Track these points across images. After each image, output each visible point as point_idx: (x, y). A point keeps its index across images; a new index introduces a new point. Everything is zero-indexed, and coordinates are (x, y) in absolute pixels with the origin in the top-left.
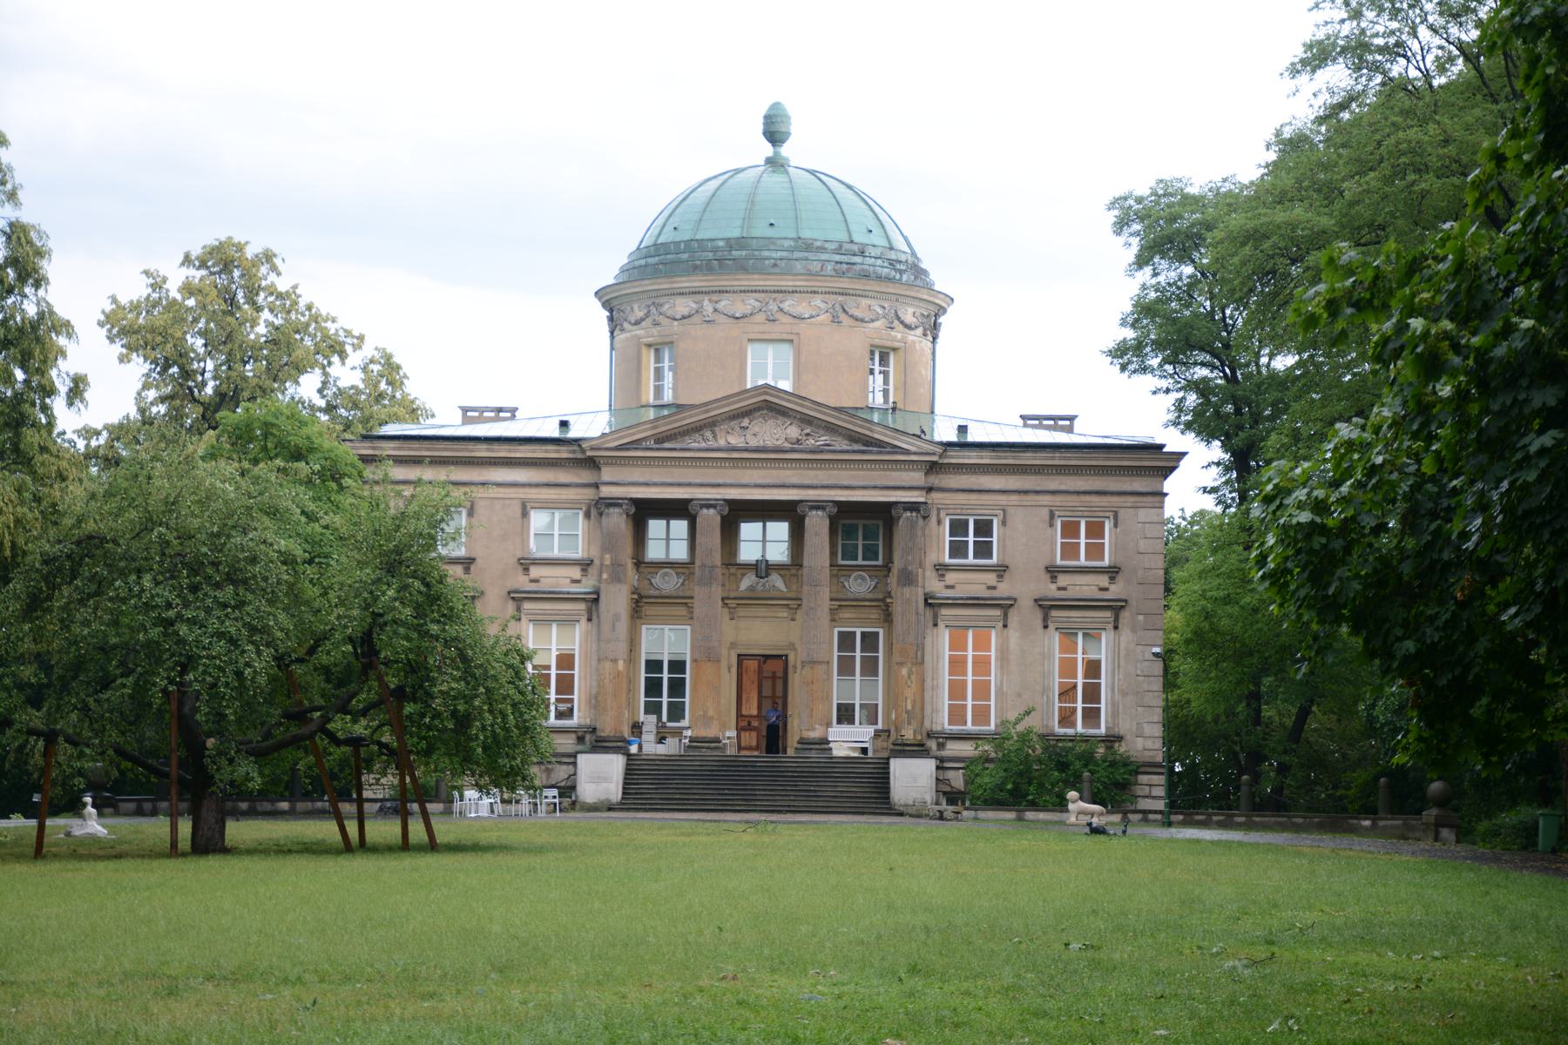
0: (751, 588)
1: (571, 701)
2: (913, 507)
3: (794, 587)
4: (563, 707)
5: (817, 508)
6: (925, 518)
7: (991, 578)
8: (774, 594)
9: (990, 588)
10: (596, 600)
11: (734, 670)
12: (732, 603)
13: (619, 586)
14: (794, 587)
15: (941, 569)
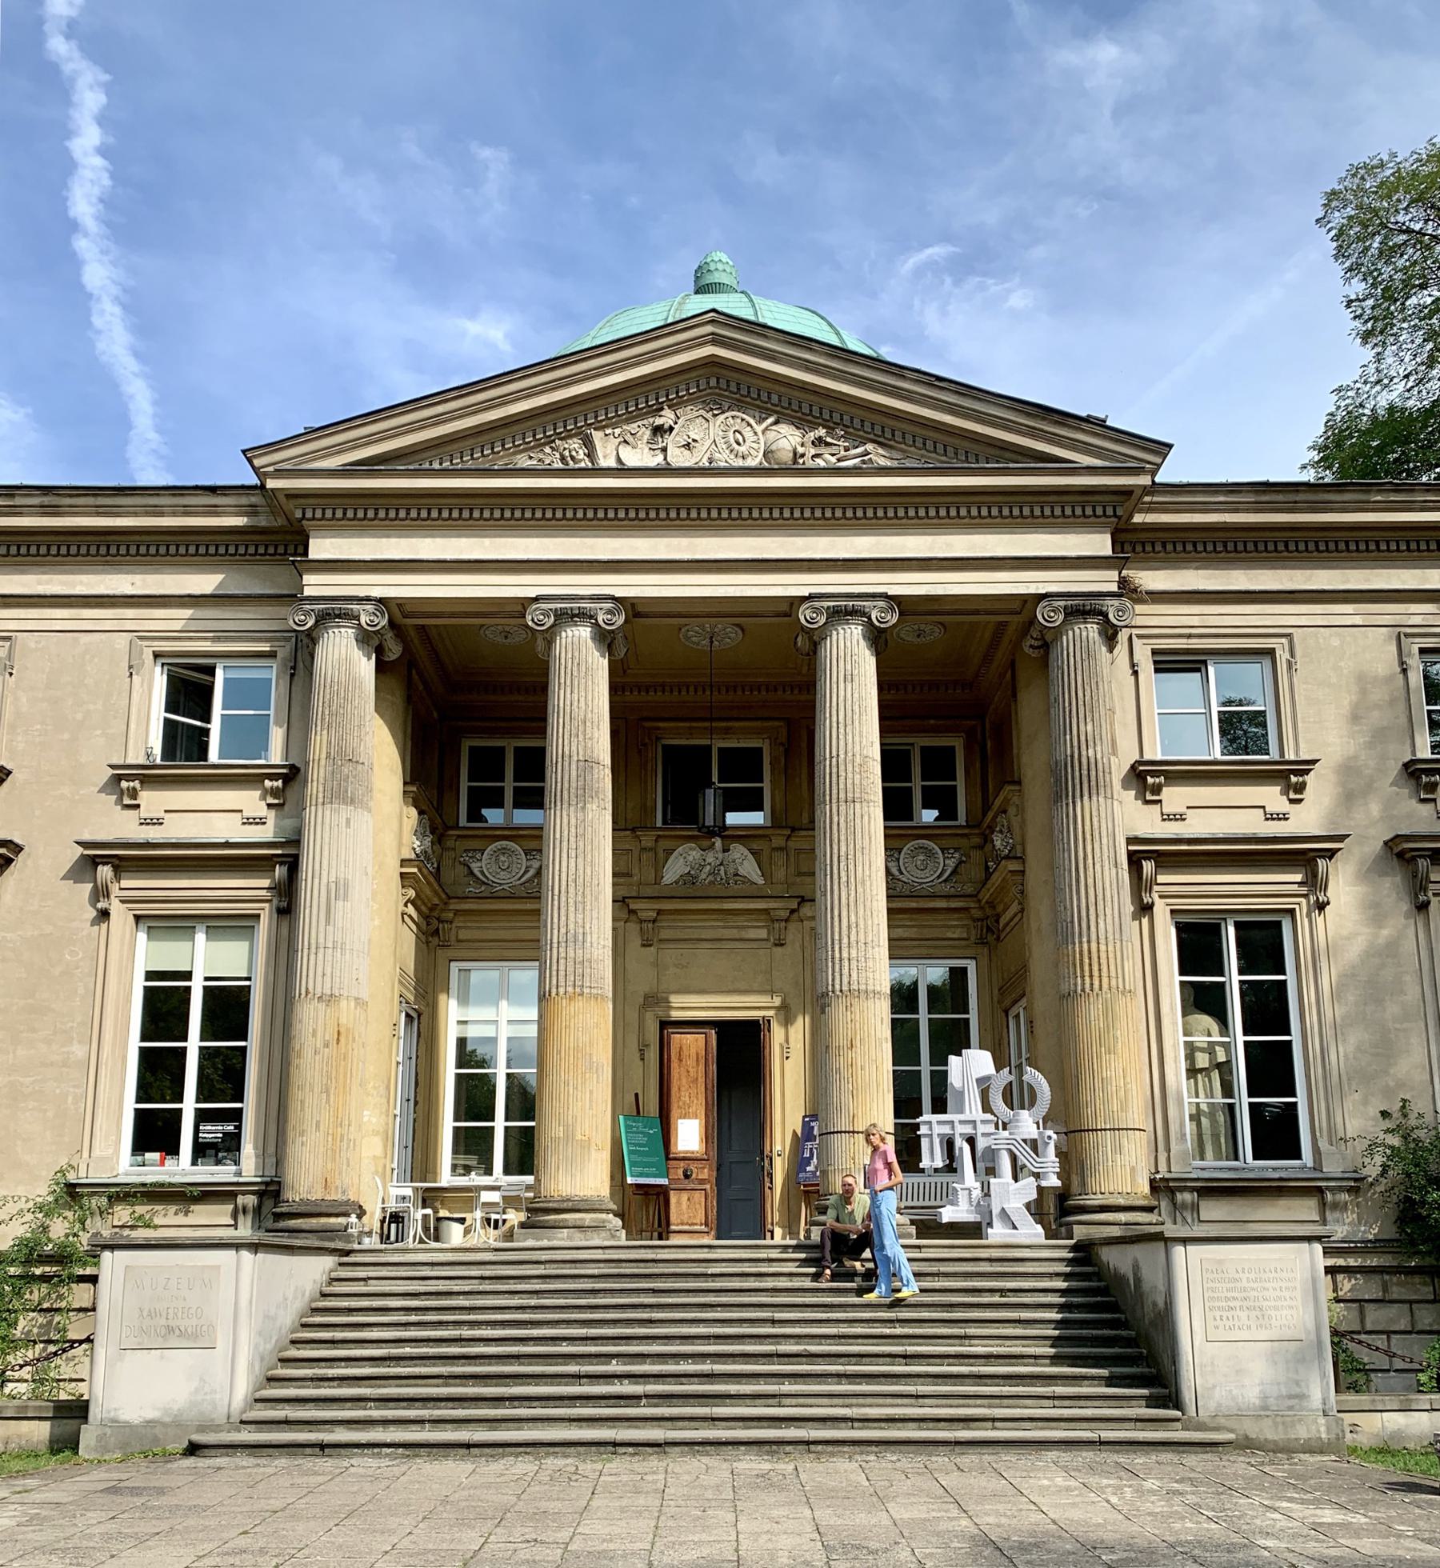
0: (689, 879)
1: (236, 1116)
2: (1083, 608)
3: (780, 874)
4: (212, 1132)
5: (854, 612)
6: (1110, 636)
7: (1271, 796)
8: (736, 889)
9: (1271, 817)
10: (293, 865)
11: (653, 1054)
12: (646, 909)
13: (345, 811)
14: (780, 874)
15: (1146, 778)
